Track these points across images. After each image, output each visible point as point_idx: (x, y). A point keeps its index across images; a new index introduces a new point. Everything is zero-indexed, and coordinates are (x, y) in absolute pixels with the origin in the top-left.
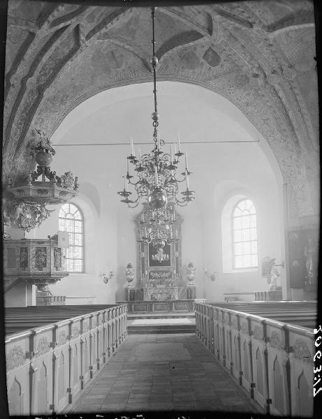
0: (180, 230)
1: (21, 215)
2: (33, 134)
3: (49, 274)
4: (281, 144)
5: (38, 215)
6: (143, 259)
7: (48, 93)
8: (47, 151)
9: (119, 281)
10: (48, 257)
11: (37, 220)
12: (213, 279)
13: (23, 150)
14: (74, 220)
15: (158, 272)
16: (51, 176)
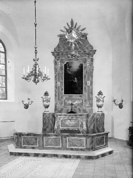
0: (92, 60)
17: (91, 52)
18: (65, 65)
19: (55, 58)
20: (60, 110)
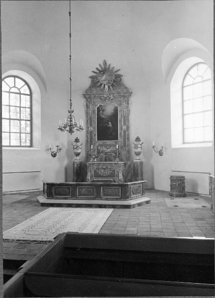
0: (128, 103)
6: (91, 132)
9: (69, 156)
12: (161, 154)
14: (20, 94)
15: (106, 146)
17: (126, 95)
18: (98, 108)
19: (87, 101)
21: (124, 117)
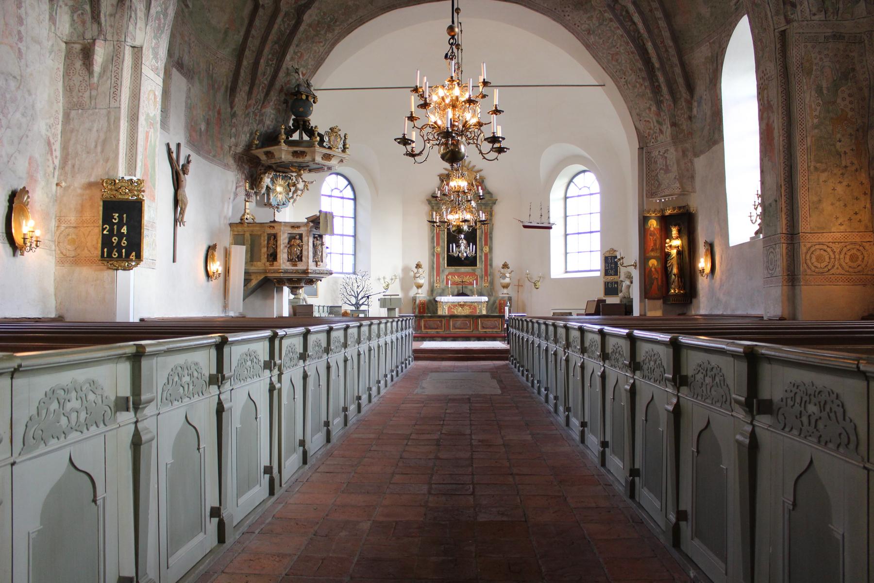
1: (268, 188)
2: (288, 74)
3: (305, 272)
4: (636, 90)
5: (293, 189)
7: (306, 17)
8: (307, 97)
10: (305, 247)
11: (291, 194)
13: (274, 96)
16: (311, 132)
20: (440, 291)
21: (486, 234)
